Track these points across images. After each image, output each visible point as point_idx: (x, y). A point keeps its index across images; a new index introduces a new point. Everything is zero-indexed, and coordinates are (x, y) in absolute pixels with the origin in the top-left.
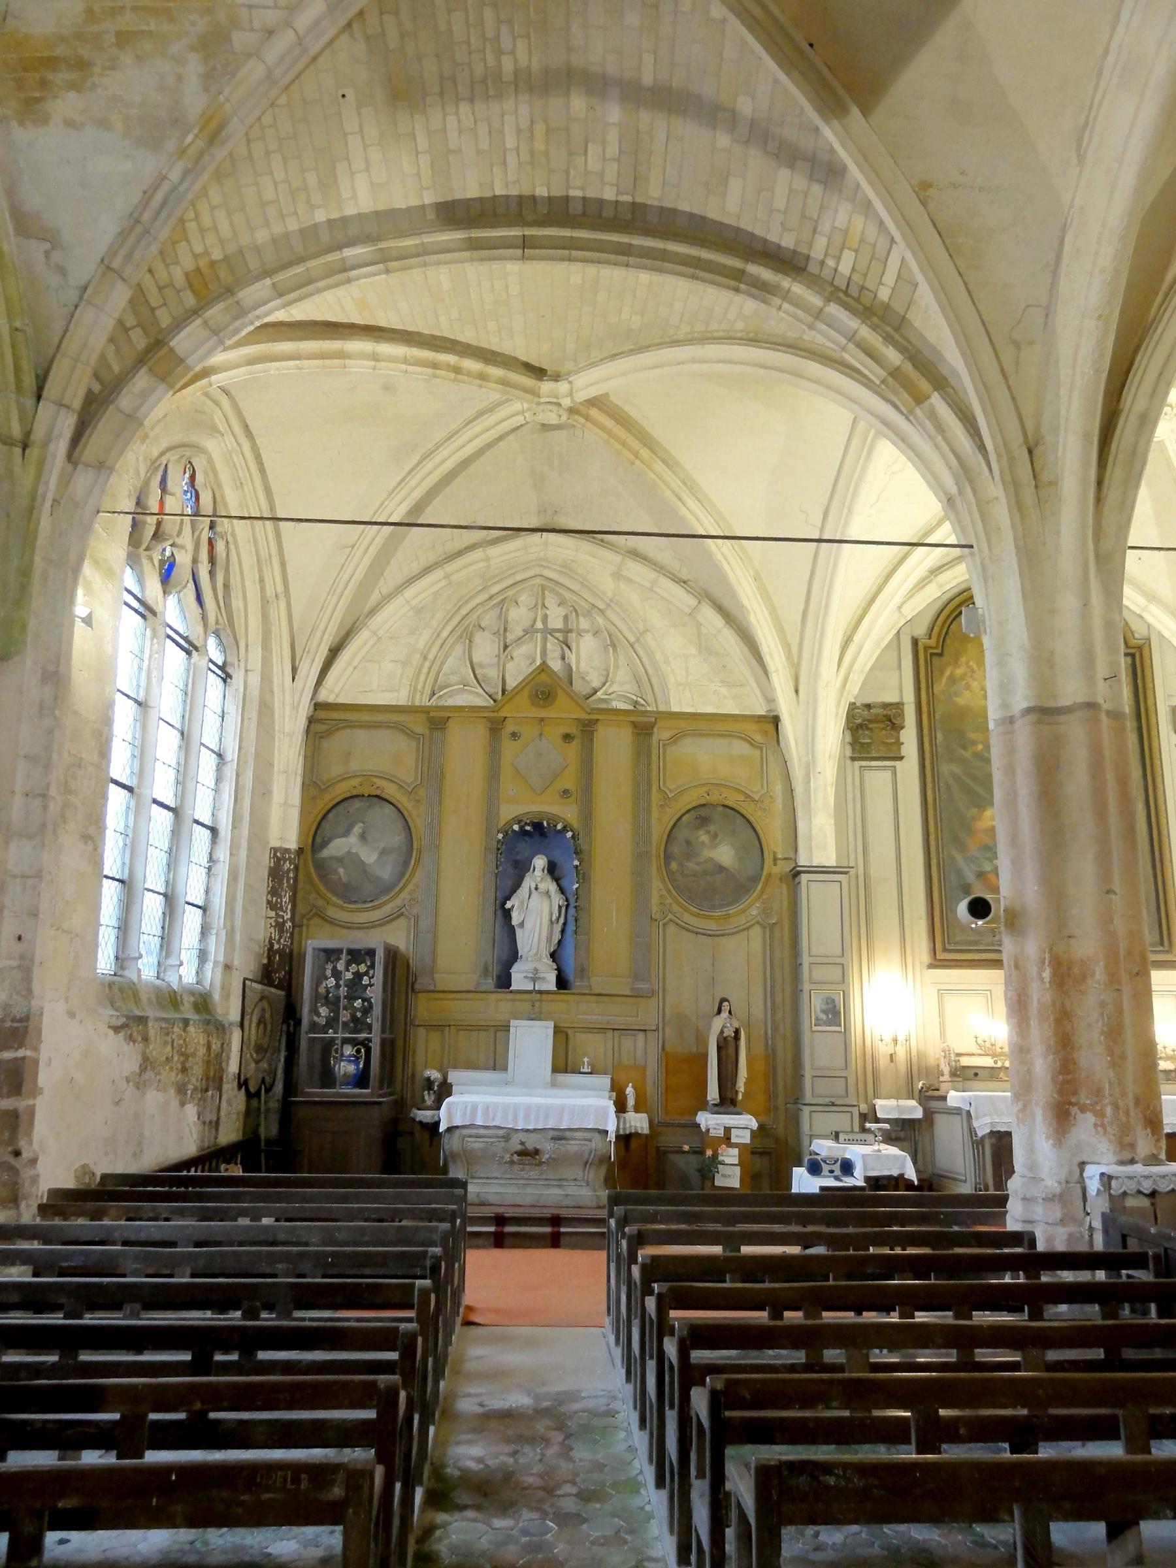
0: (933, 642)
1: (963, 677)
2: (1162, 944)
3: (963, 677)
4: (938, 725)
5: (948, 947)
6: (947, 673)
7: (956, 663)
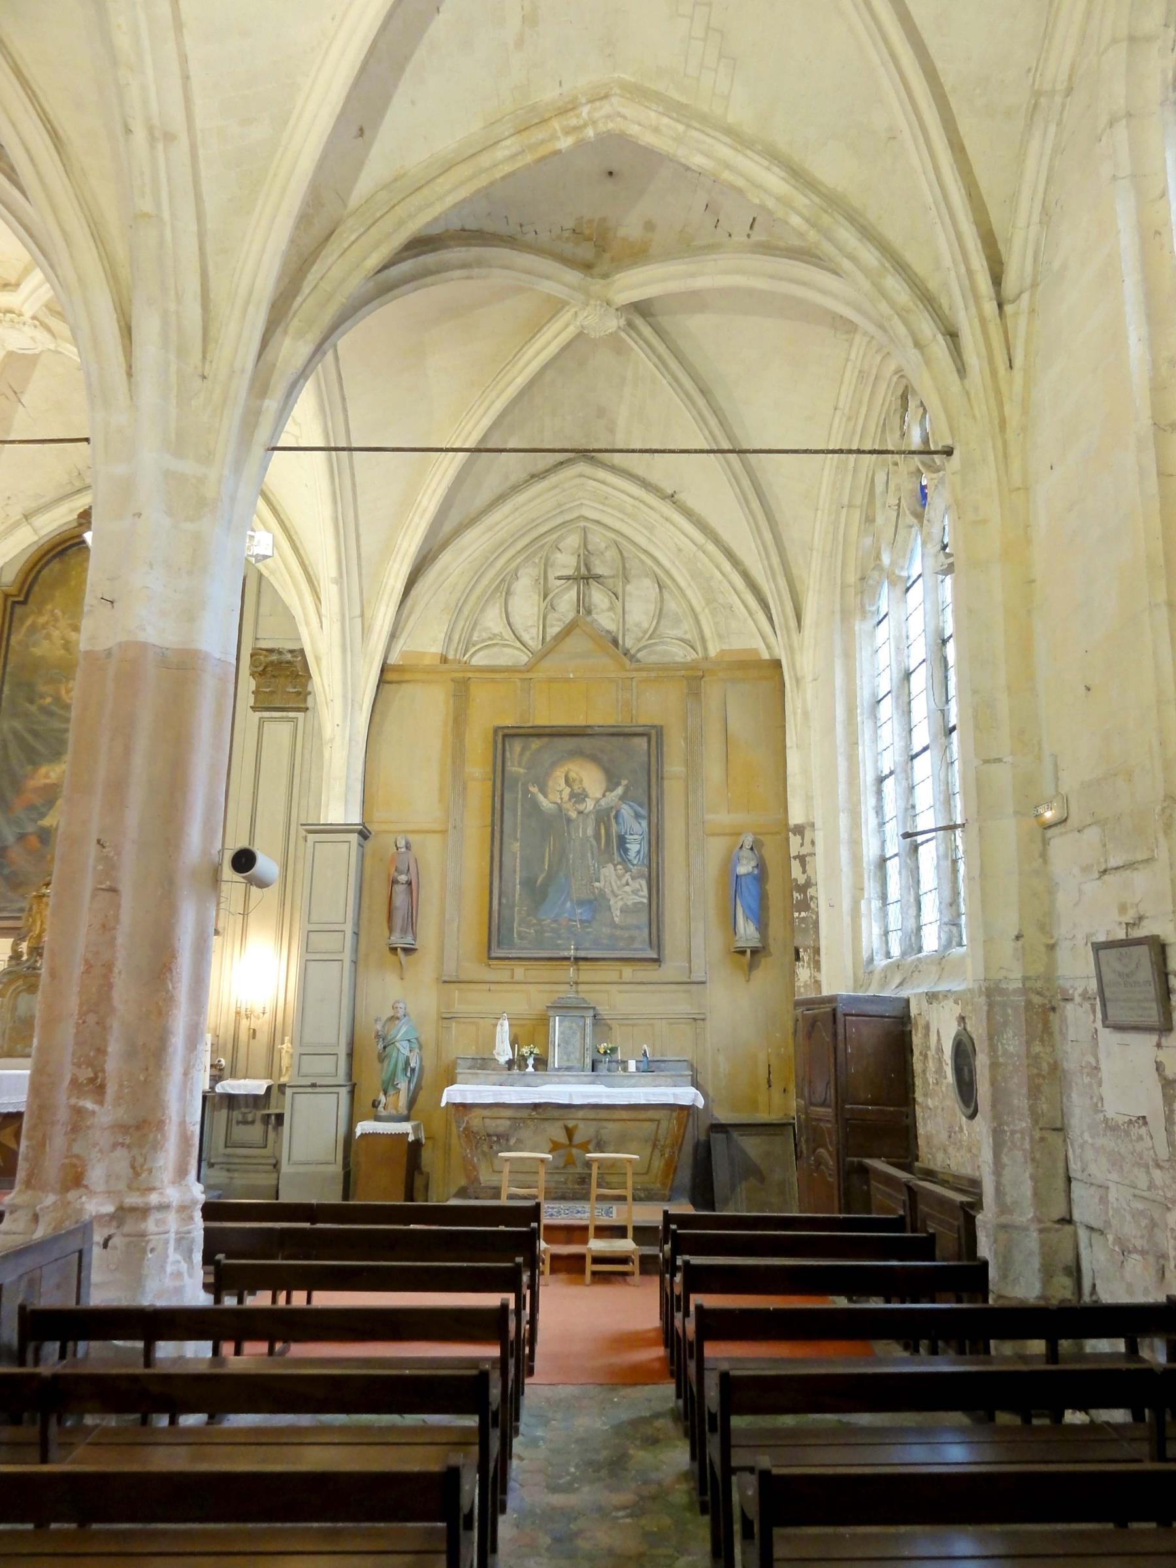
1: (44, 626)
3: (44, 626)
6: (29, 622)
7: (40, 613)
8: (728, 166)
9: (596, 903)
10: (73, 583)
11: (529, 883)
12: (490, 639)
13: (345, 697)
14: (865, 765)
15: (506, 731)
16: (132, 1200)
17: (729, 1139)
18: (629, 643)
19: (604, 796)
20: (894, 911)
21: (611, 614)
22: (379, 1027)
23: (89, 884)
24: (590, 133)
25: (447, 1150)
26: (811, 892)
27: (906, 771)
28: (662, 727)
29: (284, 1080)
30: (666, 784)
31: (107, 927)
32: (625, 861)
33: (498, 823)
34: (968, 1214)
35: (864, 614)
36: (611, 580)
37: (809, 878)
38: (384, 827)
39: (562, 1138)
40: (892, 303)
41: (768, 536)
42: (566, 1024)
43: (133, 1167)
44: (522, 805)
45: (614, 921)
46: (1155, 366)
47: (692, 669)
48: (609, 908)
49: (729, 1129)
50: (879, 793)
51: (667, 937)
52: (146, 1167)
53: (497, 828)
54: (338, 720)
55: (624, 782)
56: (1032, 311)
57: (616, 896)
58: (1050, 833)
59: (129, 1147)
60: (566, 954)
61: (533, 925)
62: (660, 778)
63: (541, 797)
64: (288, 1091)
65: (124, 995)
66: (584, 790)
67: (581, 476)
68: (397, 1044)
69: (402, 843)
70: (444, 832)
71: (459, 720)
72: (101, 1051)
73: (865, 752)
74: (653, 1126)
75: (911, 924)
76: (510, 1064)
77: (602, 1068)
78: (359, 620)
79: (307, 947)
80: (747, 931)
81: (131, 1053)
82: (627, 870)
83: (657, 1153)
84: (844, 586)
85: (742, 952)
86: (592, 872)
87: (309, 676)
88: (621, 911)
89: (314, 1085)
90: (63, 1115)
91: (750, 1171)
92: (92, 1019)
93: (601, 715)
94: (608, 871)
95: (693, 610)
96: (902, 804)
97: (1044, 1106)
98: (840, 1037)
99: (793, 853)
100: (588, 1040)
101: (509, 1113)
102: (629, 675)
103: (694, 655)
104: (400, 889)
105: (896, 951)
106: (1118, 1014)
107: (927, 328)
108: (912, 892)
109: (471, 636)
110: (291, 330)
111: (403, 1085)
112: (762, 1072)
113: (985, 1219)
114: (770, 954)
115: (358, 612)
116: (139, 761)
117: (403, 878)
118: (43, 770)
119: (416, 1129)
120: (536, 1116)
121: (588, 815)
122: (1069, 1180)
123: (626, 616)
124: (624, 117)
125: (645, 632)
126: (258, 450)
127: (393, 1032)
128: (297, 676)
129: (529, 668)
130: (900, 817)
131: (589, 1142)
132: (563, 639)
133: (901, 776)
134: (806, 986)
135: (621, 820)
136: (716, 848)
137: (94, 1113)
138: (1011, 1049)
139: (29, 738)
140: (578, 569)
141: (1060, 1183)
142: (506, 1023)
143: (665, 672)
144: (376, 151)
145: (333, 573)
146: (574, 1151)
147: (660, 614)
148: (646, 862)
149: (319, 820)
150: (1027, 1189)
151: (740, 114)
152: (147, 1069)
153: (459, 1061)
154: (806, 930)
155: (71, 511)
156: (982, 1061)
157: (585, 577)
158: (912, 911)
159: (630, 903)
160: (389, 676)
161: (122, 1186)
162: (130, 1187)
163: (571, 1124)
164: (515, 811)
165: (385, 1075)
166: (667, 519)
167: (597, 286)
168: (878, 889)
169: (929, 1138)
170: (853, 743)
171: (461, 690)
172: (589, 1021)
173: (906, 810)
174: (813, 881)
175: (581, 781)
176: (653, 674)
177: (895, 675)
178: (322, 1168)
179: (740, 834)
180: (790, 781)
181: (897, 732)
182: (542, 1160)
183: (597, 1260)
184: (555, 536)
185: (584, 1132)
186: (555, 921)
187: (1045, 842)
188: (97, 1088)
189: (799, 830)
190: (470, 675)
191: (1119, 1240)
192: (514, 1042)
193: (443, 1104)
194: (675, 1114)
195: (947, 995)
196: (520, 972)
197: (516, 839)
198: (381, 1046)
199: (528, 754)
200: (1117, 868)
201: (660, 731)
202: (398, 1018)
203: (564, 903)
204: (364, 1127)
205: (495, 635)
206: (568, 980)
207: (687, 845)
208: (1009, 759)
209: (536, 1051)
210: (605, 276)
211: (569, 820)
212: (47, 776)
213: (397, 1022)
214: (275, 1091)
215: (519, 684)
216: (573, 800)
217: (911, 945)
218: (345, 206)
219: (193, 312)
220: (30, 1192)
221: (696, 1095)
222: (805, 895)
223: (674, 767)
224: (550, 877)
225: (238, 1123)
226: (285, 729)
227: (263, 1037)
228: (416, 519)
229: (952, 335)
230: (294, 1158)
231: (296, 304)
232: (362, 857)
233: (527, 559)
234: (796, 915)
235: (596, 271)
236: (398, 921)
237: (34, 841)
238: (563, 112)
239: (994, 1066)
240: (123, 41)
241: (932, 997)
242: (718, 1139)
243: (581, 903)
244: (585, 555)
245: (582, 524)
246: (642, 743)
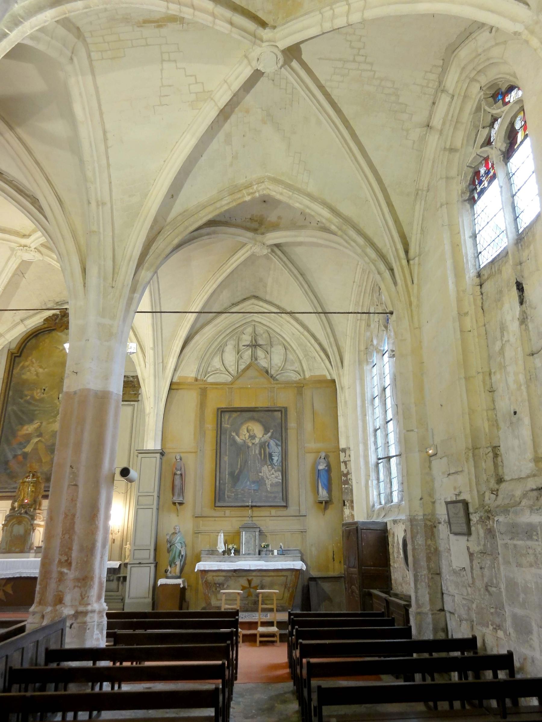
1: (28, 367)
3: (28, 367)
4: (11, 388)
6: (21, 365)
7: (26, 360)
8: (308, 207)
9: (260, 482)
10: (40, 348)
11: (232, 474)
12: (216, 371)
13: (155, 396)
14: (369, 424)
15: (222, 410)
16: (81, 609)
17: (317, 584)
18: (273, 372)
19: (263, 436)
20: (382, 485)
21: (265, 360)
22: (168, 537)
23: (66, 484)
24: (257, 195)
25: (197, 590)
26: (349, 476)
27: (384, 428)
28: (287, 407)
29: (127, 561)
30: (289, 431)
31: (73, 500)
32: (272, 464)
33: (218, 448)
34: (407, 608)
35: (368, 363)
36: (265, 346)
37: (348, 470)
38: (171, 451)
39: (246, 584)
40: (369, 258)
41: (329, 330)
42: (248, 535)
43: (81, 596)
44: (229, 441)
45: (268, 490)
46: (458, 292)
47: (298, 383)
48: (265, 484)
49: (317, 580)
50: (375, 436)
51: (290, 496)
52: (86, 595)
53: (218, 451)
54: (152, 405)
55: (271, 431)
56: (419, 264)
57: (268, 479)
58: (432, 458)
59: (80, 587)
60: (247, 504)
61: (233, 492)
62: (286, 429)
63: (237, 437)
64: (129, 566)
65: (79, 527)
66: (255, 434)
67: (253, 304)
68: (176, 545)
69: (178, 457)
70: (196, 452)
71: (202, 405)
72: (70, 549)
73: (369, 418)
74: (284, 578)
75: (388, 491)
76: (224, 552)
77: (263, 553)
78: (162, 364)
79: (138, 503)
80: (323, 493)
81: (81, 549)
82: (273, 468)
83: (286, 590)
84: (359, 351)
85: (321, 503)
86: (258, 469)
87: (140, 387)
88: (271, 486)
89: (140, 563)
90: (55, 575)
91: (327, 598)
92: (67, 536)
93: (261, 402)
94: (265, 469)
95: (299, 358)
96: (383, 442)
97: (432, 565)
98: (360, 539)
99: (342, 460)
100: (257, 541)
101: (224, 574)
102: (273, 386)
103: (300, 377)
104: (177, 478)
105: (383, 502)
106: (454, 529)
107: (382, 267)
108: (388, 478)
109: (207, 369)
110: (144, 268)
111: (178, 563)
112: (331, 554)
113: (412, 610)
114: (332, 503)
115: (161, 361)
116: (86, 435)
117: (179, 472)
118: (25, 427)
119: (183, 582)
120: (236, 575)
121: (256, 445)
122: (443, 594)
123: (272, 361)
124: (270, 190)
125: (280, 368)
126: (132, 313)
127: (174, 539)
128: (135, 387)
129: (232, 383)
130: (383, 446)
131: (257, 586)
132: (246, 371)
133: (383, 430)
134: (348, 517)
135: (270, 447)
136: (310, 458)
137: (67, 573)
138: (420, 542)
139: (20, 413)
140: (252, 341)
141: (439, 595)
142: (222, 535)
143: (288, 384)
144: (178, 202)
145: (151, 345)
146: (252, 590)
147: (286, 360)
148: (281, 464)
149: (143, 447)
150: (427, 598)
151: (311, 188)
152: (87, 556)
153: (202, 552)
154: (347, 493)
155: (41, 318)
156: (409, 547)
157: (254, 345)
158: (389, 486)
159: (274, 482)
160: (174, 387)
161: (77, 603)
162: (80, 604)
163: (250, 578)
164: (226, 444)
165: (171, 559)
166: (288, 322)
167: (259, 237)
168: (376, 476)
169: (396, 580)
170: (364, 415)
171: (203, 392)
172: (257, 533)
173: (385, 444)
174: (350, 472)
175: (253, 430)
176: (283, 386)
177: (379, 389)
178: (142, 600)
179: (320, 452)
180: (340, 430)
181: (381, 412)
182: (239, 593)
183: (262, 635)
184: (242, 328)
185: (256, 581)
186: (242, 490)
187: (430, 462)
188: (68, 564)
189: (344, 450)
190: (207, 386)
191: (459, 616)
192: (225, 543)
193: (196, 570)
194: (294, 573)
195: (400, 521)
196: (228, 512)
197: (226, 455)
198: (169, 545)
199: (231, 419)
200: (453, 473)
201: (286, 409)
202: (176, 533)
203: (246, 482)
204: (161, 581)
205: (218, 369)
206: (248, 516)
207: (298, 456)
208: (416, 430)
209: (235, 547)
210: (263, 234)
211: (248, 447)
212: (27, 430)
213: (176, 535)
214: (122, 566)
215: (227, 390)
216: (250, 439)
217: (388, 500)
218: (166, 221)
219: (110, 263)
220: (41, 606)
221: (302, 565)
222: (347, 478)
223: (292, 424)
224: (241, 472)
226: (130, 409)
227: (118, 543)
228: (186, 323)
229: (391, 270)
231: (147, 258)
232: (161, 464)
233: (230, 338)
234: (343, 486)
235: (259, 231)
236: (177, 490)
237: (20, 458)
238: (247, 187)
239: (414, 549)
240: (89, 174)
241: (395, 522)
242: (312, 583)
243: (254, 482)
244: (255, 336)
245: (253, 323)
246: (278, 414)
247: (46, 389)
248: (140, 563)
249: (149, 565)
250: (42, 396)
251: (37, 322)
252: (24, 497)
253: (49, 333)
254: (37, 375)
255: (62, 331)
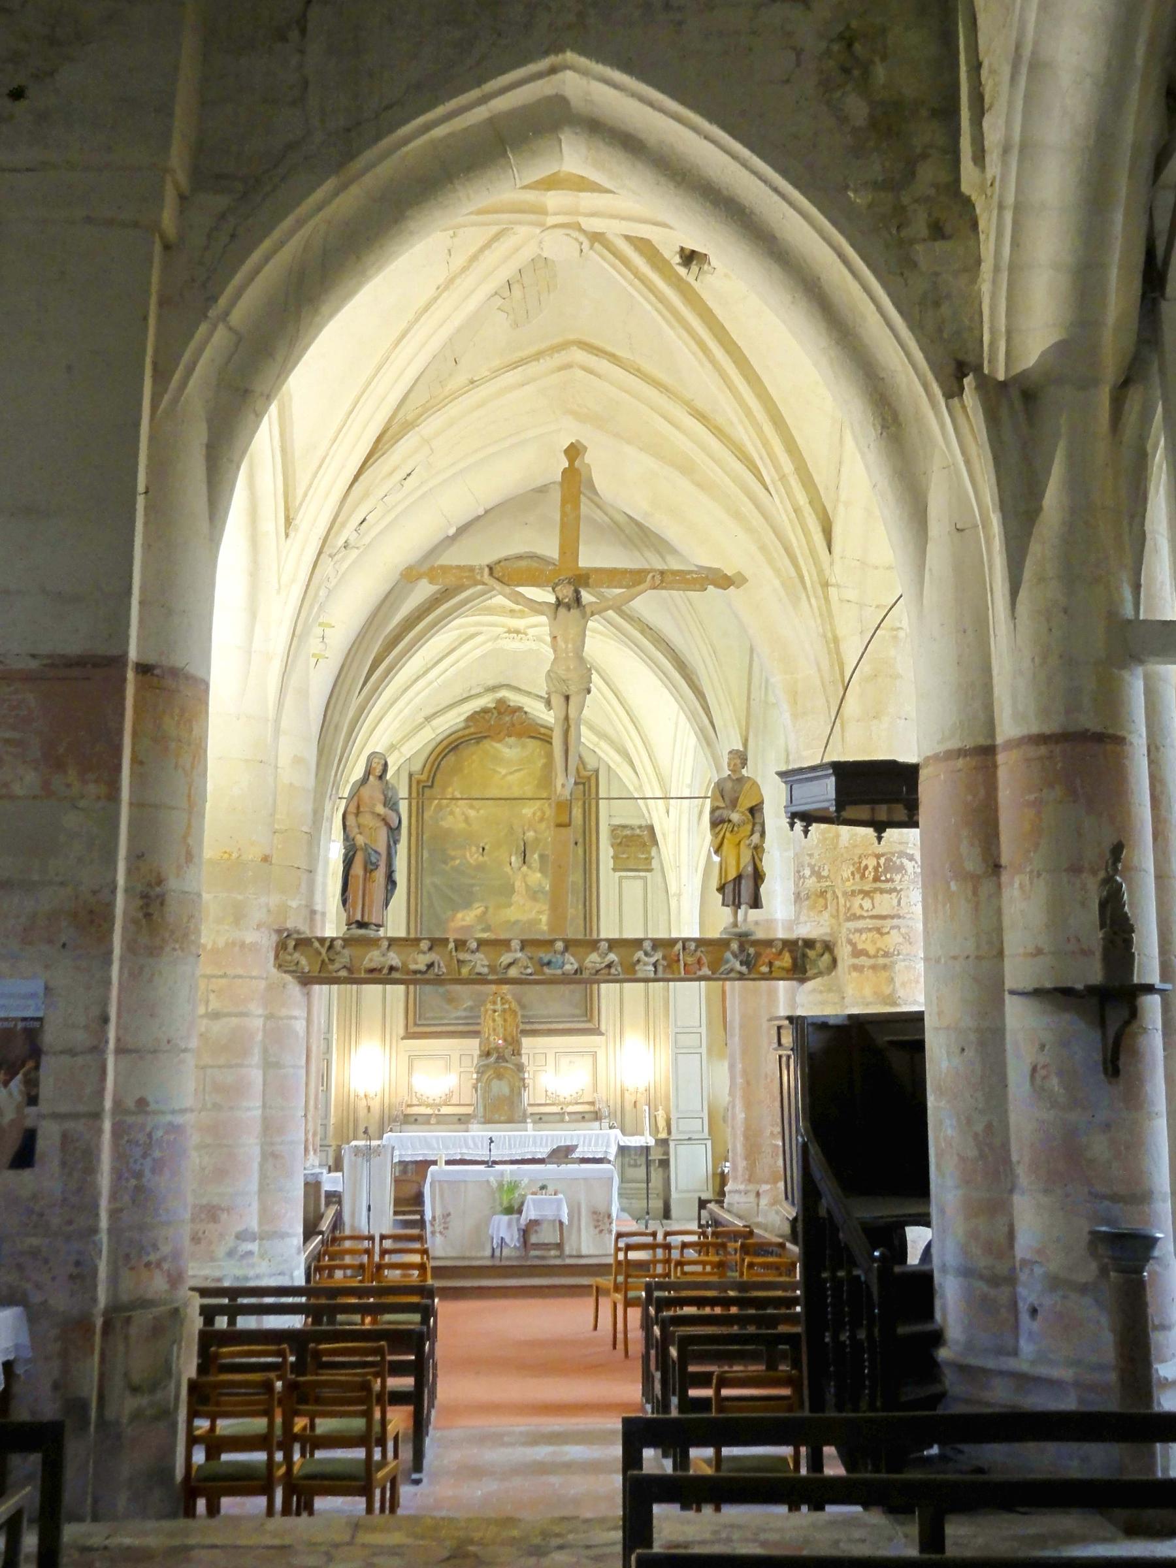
0: (424, 777)
2: (586, 1016)
5: (418, 1022)
10: (466, 771)
89: (690, 1139)
118: (460, 915)
212: (463, 920)
225: (630, 1166)
226: (639, 884)
230: (680, 1187)
247: (487, 847)
248: (690, 1139)
249: (705, 1142)
250: (481, 858)
251: (452, 723)
252: (489, 1035)
253: (478, 743)
254: (467, 820)
255: (500, 741)
